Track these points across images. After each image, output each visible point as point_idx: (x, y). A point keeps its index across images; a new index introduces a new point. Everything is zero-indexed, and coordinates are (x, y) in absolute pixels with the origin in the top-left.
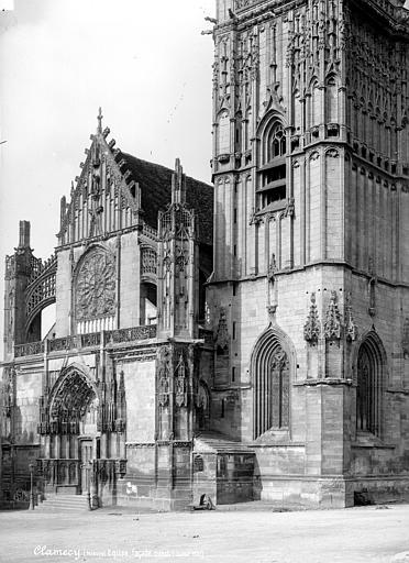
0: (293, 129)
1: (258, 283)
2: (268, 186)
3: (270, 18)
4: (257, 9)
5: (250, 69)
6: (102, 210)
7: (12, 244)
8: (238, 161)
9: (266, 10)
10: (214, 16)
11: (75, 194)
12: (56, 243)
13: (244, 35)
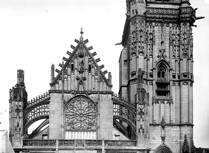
1: (157, 127)
2: (160, 89)
4: (158, 16)
6: (85, 79)
7: (14, 82)
11: (64, 67)
12: (49, 88)
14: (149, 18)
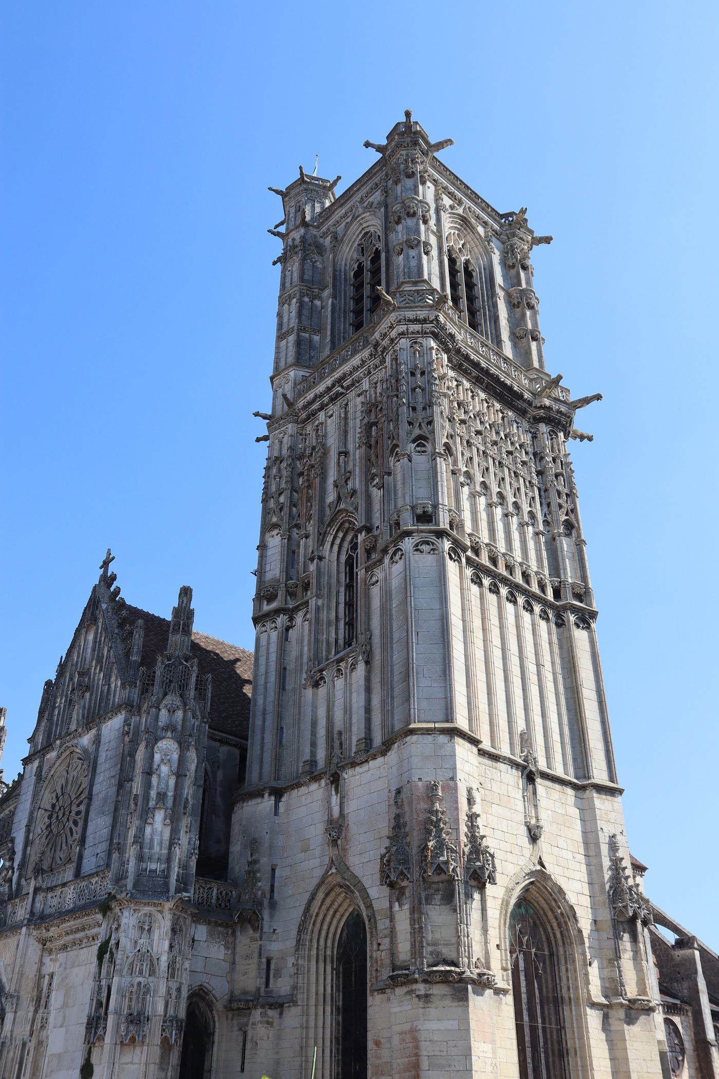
0: (369, 529)
3: (338, 395)
4: (321, 388)
5: (312, 466)
8: (291, 594)
9: (333, 385)
10: (269, 413)
13: (309, 428)
14: (305, 407)
